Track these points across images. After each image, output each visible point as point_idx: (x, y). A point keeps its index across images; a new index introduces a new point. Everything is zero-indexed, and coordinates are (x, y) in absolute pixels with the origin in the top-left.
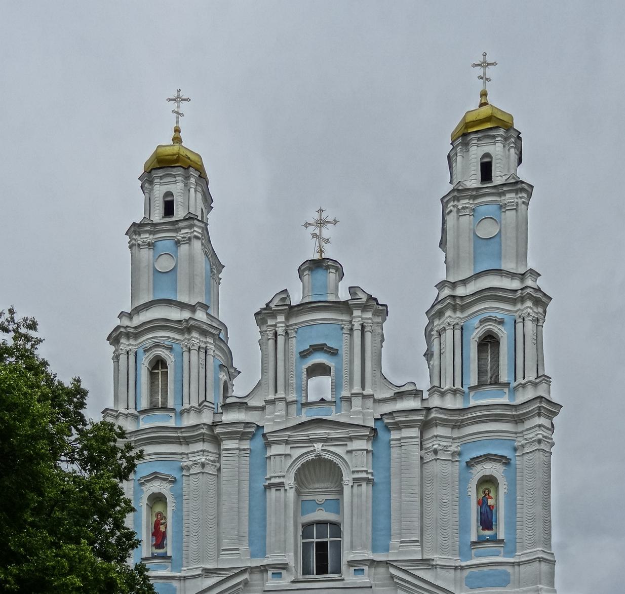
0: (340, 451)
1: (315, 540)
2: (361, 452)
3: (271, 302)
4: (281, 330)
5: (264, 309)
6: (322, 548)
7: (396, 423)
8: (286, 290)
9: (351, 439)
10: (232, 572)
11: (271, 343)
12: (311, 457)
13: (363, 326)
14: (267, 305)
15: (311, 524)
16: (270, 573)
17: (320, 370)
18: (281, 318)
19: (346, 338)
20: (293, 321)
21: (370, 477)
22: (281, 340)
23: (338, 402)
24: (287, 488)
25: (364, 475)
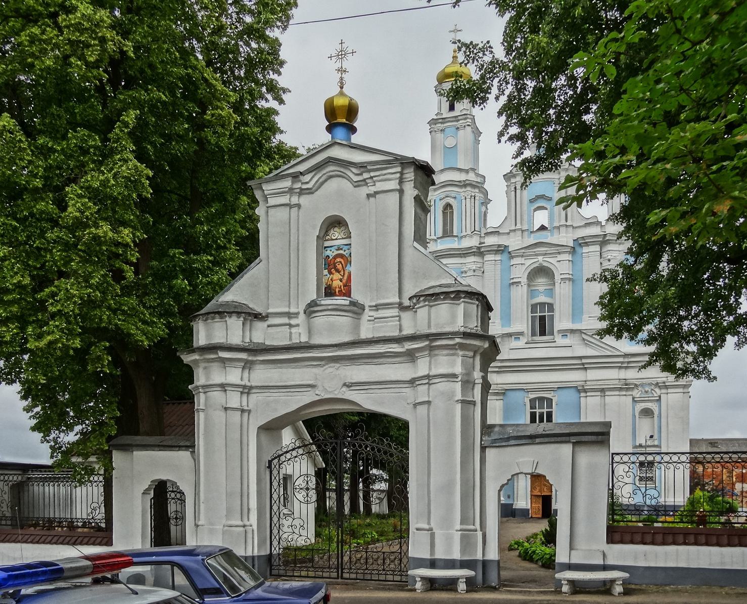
1: (538, 314)
7: (586, 243)
9: (559, 253)
21: (571, 276)
25: (567, 276)
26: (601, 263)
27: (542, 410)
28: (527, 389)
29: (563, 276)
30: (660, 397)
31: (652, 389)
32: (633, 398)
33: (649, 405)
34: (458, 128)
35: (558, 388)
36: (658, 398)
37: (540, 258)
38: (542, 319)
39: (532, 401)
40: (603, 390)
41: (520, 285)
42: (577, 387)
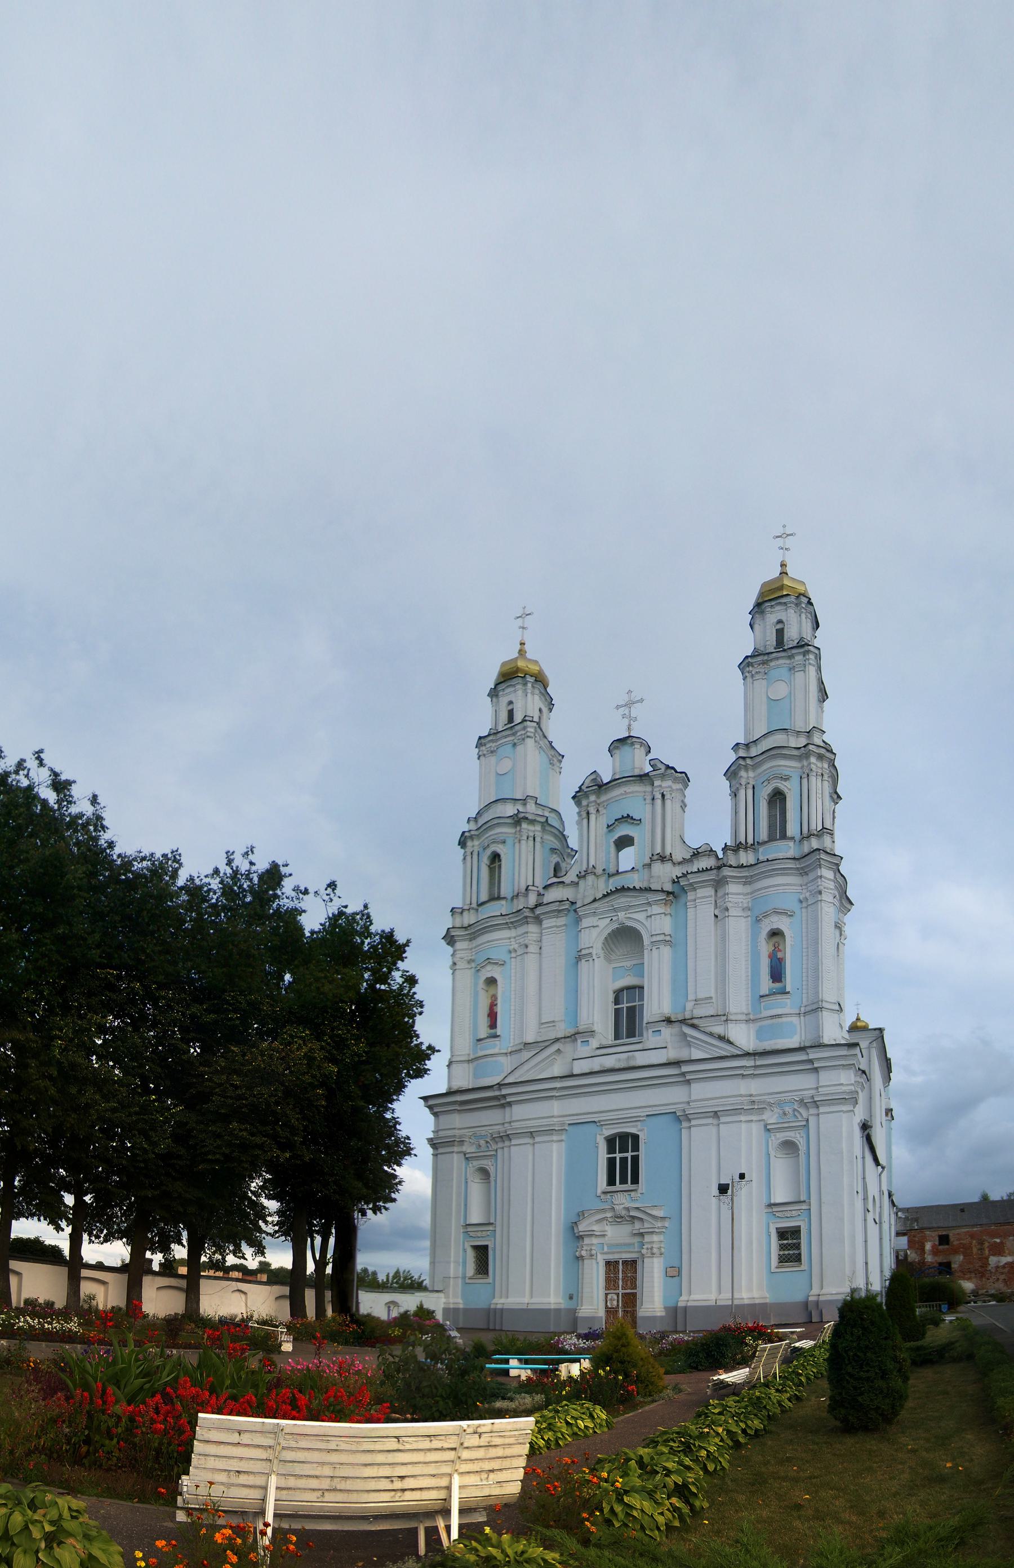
0: (641, 916)
2: (659, 916)
3: (583, 784)
4: (592, 810)
5: (577, 792)
6: (631, 1010)
7: (691, 884)
8: (595, 771)
9: (649, 904)
10: (547, 1044)
11: (585, 821)
12: (615, 926)
13: (663, 796)
14: (580, 788)
15: (621, 990)
16: (579, 1041)
17: (624, 842)
18: (593, 798)
19: (649, 807)
20: (603, 798)
21: (668, 938)
22: (593, 817)
23: (641, 869)
24: (594, 958)
25: (662, 937)
26: (716, 916)
27: (625, 1155)
28: (599, 1122)
29: (654, 939)
30: (807, 1120)
31: (795, 1110)
32: (766, 1126)
33: (790, 1135)
34: (515, 745)
35: (647, 1116)
36: (804, 1123)
37: (621, 915)
38: (631, 1010)
39: (611, 1141)
40: (716, 1114)
41: (591, 959)
42: (675, 1112)
